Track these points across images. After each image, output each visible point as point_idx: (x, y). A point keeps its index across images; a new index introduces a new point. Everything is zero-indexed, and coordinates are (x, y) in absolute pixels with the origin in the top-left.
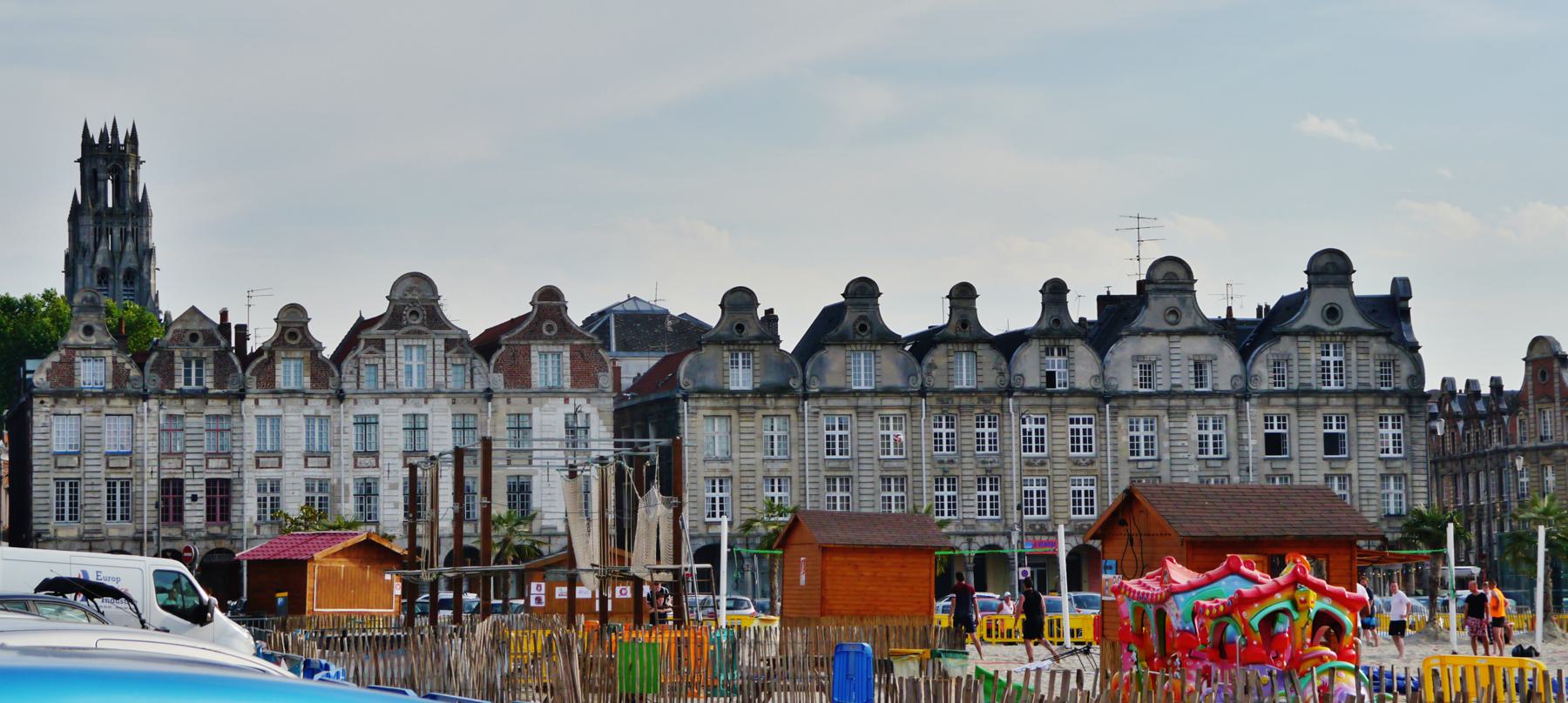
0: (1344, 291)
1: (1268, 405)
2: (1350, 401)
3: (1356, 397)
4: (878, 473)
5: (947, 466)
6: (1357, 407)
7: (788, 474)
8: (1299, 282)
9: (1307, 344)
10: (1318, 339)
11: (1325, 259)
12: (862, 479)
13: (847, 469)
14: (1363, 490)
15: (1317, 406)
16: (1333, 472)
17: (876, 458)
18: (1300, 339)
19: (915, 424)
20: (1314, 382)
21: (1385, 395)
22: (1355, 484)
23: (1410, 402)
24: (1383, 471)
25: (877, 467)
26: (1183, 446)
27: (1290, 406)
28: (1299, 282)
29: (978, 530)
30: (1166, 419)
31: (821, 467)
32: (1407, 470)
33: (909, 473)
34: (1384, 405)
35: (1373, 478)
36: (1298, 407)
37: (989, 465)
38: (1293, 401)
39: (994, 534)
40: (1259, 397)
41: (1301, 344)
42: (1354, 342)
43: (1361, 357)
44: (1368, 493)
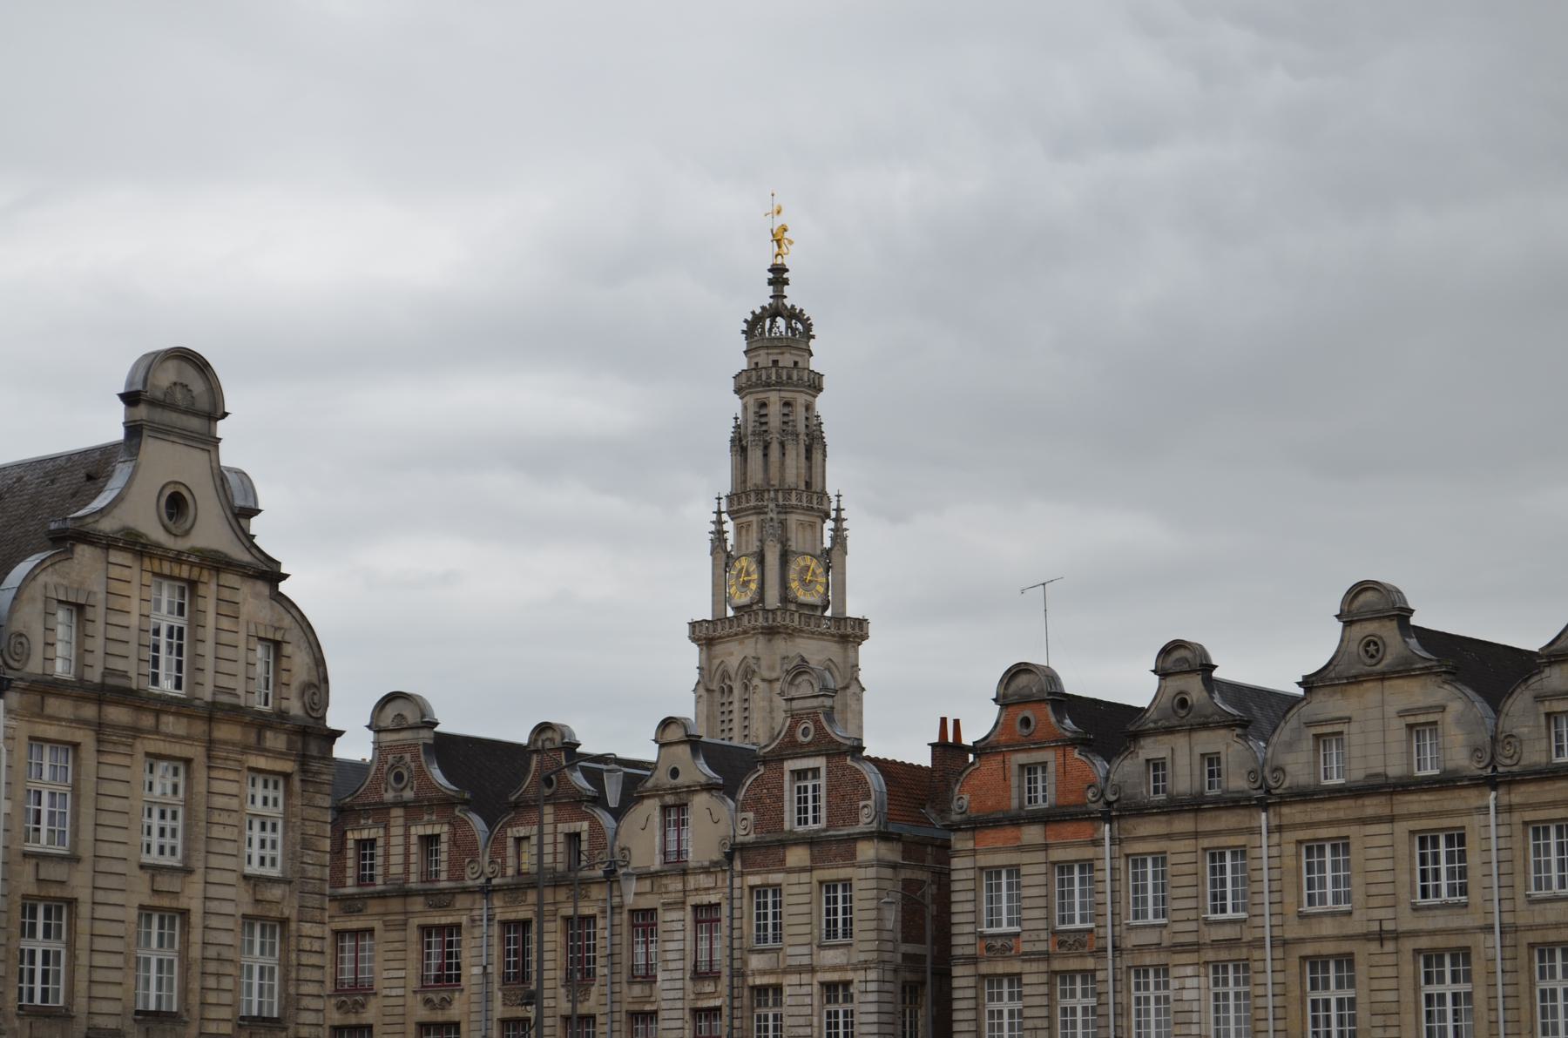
0: (199, 457)
1: (40, 714)
2: (199, 728)
3: (210, 720)
6: (210, 744)
8: (109, 426)
9: (126, 573)
10: (147, 562)
11: (166, 376)
14: (212, 952)
15: (136, 732)
16: (156, 902)
18: (116, 557)
20: (133, 670)
21: (261, 723)
22: (196, 936)
23: (305, 745)
24: (249, 910)
27: (81, 722)
28: (109, 426)
32: (289, 911)
34: (260, 749)
35: (230, 924)
36: (100, 728)
38: (89, 711)
40: (24, 690)
41: (115, 572)
42: (213, 586)
43: (226, 623)
44: (219, 959)
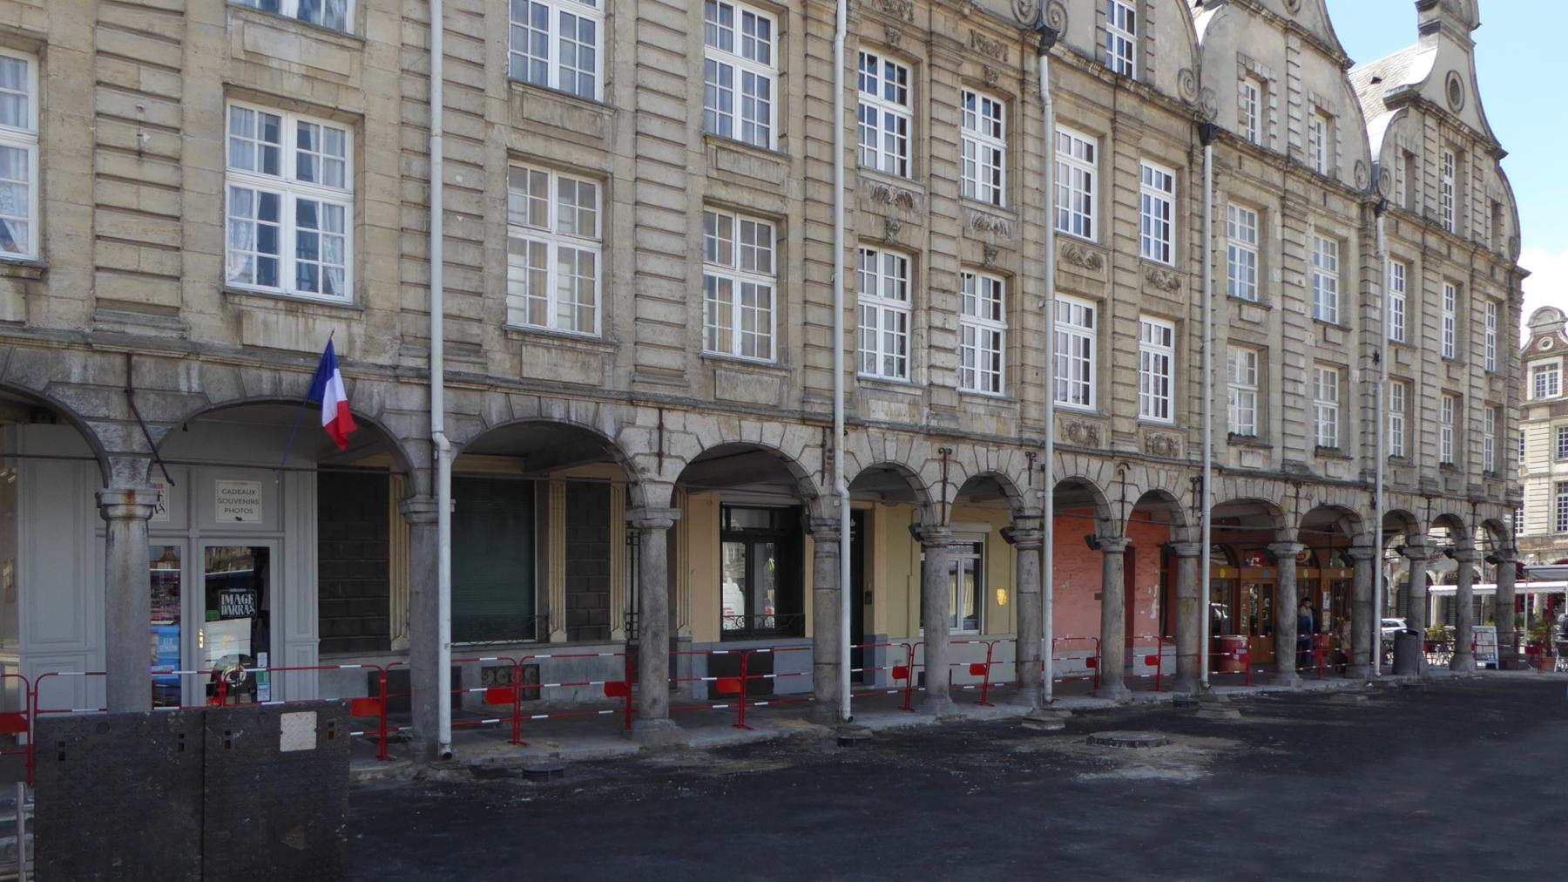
4: (699, 187)
5: (894, 212)
7: (351, 103)
12: (649, 194)
13: (594, 142)
17: (693, 128)
19: (815, 48)
25: (696, 163)
26: (1299, 286)
29: (965, 426)
30: (1278, 219)
31: (495, 111)
33: (794, 210)
37: (990, 238)
39: (998, 442)
